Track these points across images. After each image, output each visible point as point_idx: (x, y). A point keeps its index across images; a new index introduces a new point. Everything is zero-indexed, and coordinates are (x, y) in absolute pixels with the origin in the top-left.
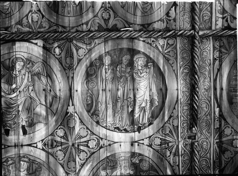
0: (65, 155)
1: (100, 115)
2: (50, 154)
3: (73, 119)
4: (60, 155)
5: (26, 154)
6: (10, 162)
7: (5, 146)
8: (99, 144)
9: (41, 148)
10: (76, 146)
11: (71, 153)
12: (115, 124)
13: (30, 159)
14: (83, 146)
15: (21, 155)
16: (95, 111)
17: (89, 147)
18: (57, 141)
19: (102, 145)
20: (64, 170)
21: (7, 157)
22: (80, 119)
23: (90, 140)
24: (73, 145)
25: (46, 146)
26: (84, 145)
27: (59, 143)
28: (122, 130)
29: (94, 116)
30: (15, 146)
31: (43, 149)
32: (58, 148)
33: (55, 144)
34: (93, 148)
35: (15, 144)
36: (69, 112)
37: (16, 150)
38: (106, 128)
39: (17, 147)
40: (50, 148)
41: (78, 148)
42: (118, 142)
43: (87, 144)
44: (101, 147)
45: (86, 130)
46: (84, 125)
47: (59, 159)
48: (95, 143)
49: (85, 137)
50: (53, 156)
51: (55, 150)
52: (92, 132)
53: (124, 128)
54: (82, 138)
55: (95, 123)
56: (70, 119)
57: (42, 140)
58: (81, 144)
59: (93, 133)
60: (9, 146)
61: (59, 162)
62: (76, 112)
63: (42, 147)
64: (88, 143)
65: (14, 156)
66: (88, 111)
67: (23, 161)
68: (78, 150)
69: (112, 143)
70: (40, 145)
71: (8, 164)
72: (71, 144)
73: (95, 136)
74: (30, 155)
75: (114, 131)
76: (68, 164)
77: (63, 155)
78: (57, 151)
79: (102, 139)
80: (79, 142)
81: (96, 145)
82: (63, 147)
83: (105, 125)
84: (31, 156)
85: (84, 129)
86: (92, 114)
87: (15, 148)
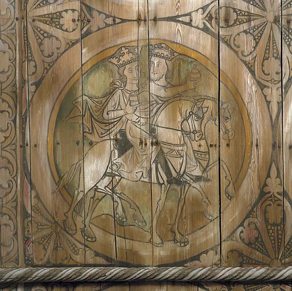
0: (257, 43)
2: (223, 39)
4: (246, 43)
5: (164, 40)
6: (126, 57)
7: (114, 21)
9: (201, 26)
10: (284, 23)
11: (271, 38)
13: (173, 52)
15: (153, 43)
18: (239, 10)
20: (255, 78)
21: (120, 44)
24: (276, 20)
25: (213, 21)
27: (244, 15)
30: (139, 20)
31: (205, 29)
32: (242, 25)
33: (234, 16)
35: (139, 15)
37: (142, 29)
39: (142, 23)
40: (222, 27)
47: (242, 52)
50: (229, 46)
51: (236, 29)
57: (204, 8)
60: (123, 21)
61: (244, 58)
63: (204, 23)
65: (135, 44)
67: (156, 55)
68: (287, 33)
70: (198, 19)
71: (121, 62)
72: (271, 18)
74: (174, 42)
76: (263, 65)
77: (253, 43)
78: (239, 34)
82: (253, 24)
84: (177, 43)
87: (139, 25)
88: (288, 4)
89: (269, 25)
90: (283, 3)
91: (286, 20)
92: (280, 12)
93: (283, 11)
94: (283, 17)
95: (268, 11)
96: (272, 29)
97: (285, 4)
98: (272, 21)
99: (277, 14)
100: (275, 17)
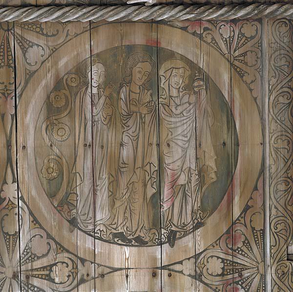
1: (80, 206)
3: (16, 214)
8: (77, 274)
10: (23, 278)
12: (115, 226)
14: (38, 277)
16: (68, 195)
17: (53, 281)
19: (83, 275)
22: (31, 213)
23: (55, 264)
24: (15, 276)
26: (40, 276)
28: (130, 241)
29: (66, 207)
34: (61, 283)
36: (5, 198)
38: (92, 234)
41: (28, 284)
42: (121, 269)
43: (48, 272)
44: (83, 281)
45: (45, 240)
46: (41, 227)
48: (66, 271)
49: (44, 256)
52: (60, 245)
53: (135, 236)
54: (36, 258)
55: (66, 224)
56: (7, 215)
58: (35, 273)
59: (61, 246)
62: (22, 196)
64: (51, 271)
66: (51, 196)
69: (107, 270)
72: (10, 275)
73: (66, 255)
75: (112, 243)
79: (83, 261)
80: (30, 268)
81: (69, 276)
83: (91, 227)
85: (42, 237)
86: (61, 204)
88: (27, 259)
89: (8, 281)
90: (22, 258)
91: (25, 277)
92: (19, 267)
93: (22, 267)
94: (22, 272)
95: (7, 266)
96: (11, 284)
97: (23, 260)
98: (11, 276)
99: (15, 270)
100: (14, 272)
